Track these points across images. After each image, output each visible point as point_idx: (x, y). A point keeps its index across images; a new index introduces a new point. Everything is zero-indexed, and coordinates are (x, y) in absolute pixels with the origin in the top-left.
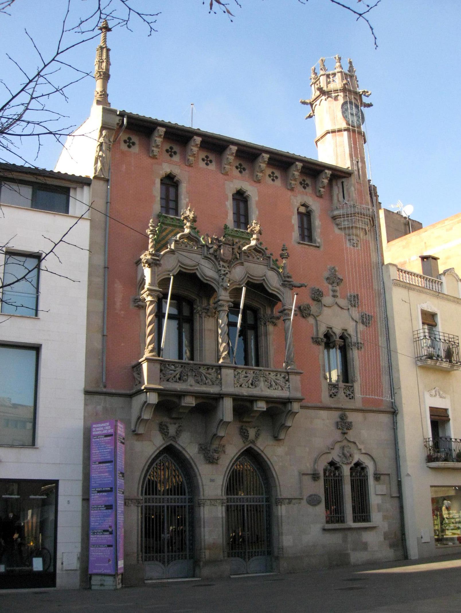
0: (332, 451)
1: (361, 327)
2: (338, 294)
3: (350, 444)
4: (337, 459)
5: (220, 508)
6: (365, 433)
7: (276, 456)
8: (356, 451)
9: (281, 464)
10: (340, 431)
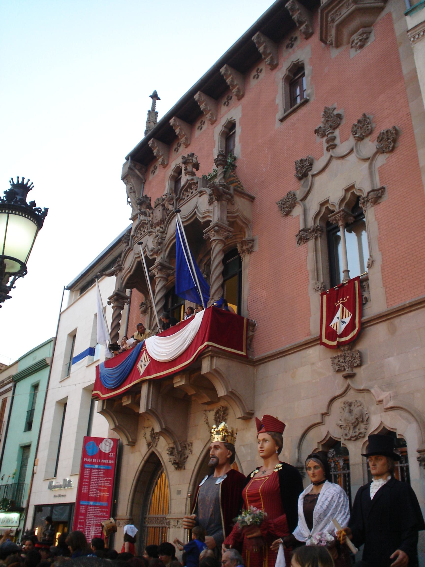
0: (327, 418)
1: (381, 160)
2: (337, 141)
3: (360, 397)
4: (336, 434)
5: (182, 530)
6: (393, 363)
7: (244, 446)
8: (373, 408)
9: (249, 459)
10: (340, 375)
